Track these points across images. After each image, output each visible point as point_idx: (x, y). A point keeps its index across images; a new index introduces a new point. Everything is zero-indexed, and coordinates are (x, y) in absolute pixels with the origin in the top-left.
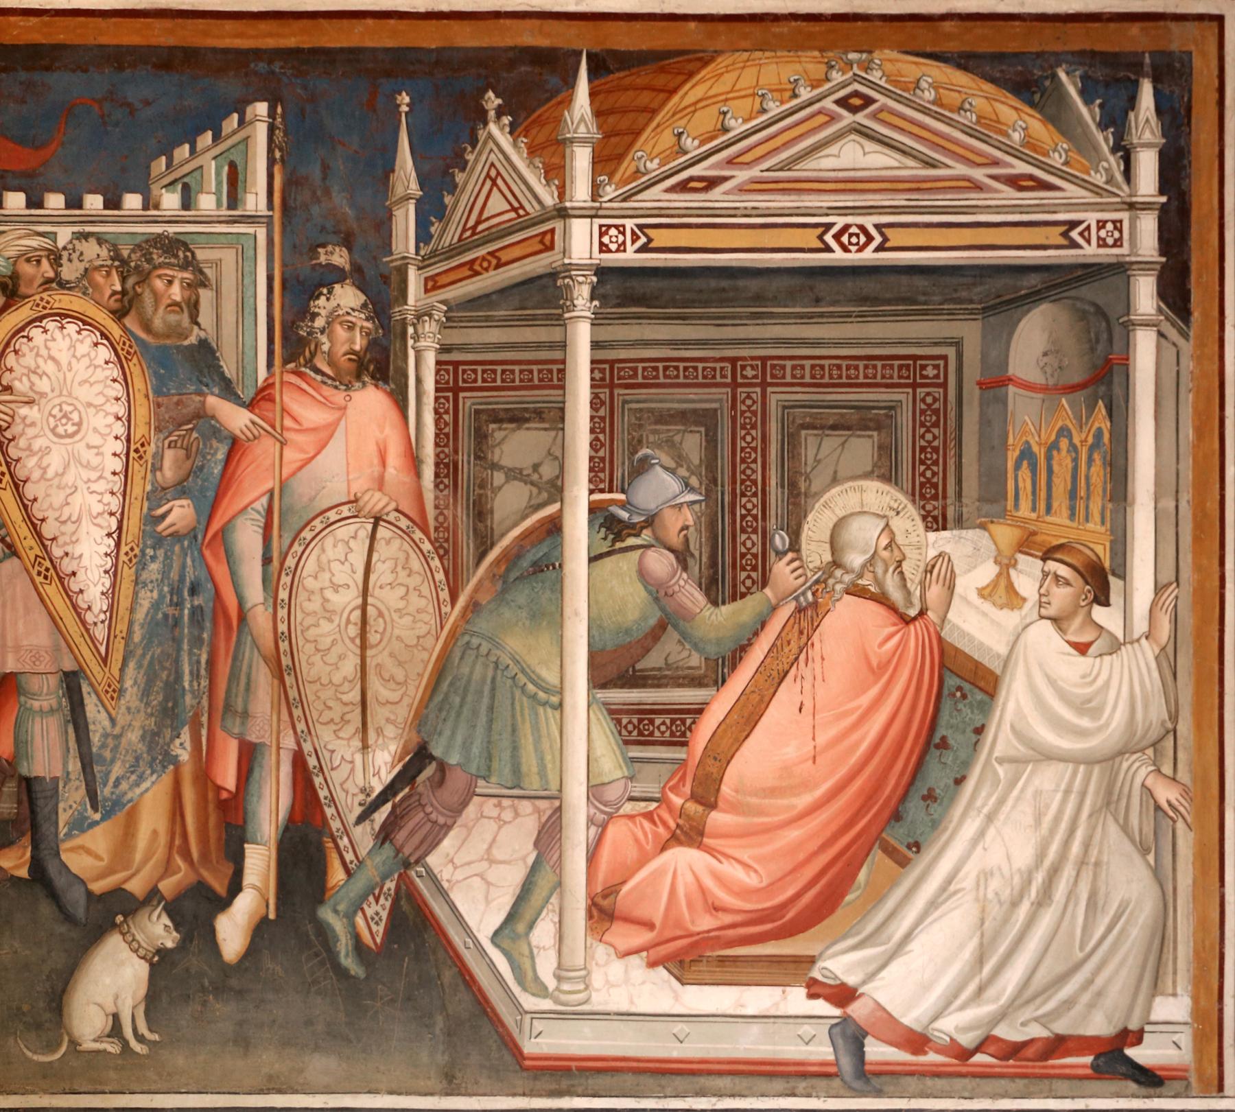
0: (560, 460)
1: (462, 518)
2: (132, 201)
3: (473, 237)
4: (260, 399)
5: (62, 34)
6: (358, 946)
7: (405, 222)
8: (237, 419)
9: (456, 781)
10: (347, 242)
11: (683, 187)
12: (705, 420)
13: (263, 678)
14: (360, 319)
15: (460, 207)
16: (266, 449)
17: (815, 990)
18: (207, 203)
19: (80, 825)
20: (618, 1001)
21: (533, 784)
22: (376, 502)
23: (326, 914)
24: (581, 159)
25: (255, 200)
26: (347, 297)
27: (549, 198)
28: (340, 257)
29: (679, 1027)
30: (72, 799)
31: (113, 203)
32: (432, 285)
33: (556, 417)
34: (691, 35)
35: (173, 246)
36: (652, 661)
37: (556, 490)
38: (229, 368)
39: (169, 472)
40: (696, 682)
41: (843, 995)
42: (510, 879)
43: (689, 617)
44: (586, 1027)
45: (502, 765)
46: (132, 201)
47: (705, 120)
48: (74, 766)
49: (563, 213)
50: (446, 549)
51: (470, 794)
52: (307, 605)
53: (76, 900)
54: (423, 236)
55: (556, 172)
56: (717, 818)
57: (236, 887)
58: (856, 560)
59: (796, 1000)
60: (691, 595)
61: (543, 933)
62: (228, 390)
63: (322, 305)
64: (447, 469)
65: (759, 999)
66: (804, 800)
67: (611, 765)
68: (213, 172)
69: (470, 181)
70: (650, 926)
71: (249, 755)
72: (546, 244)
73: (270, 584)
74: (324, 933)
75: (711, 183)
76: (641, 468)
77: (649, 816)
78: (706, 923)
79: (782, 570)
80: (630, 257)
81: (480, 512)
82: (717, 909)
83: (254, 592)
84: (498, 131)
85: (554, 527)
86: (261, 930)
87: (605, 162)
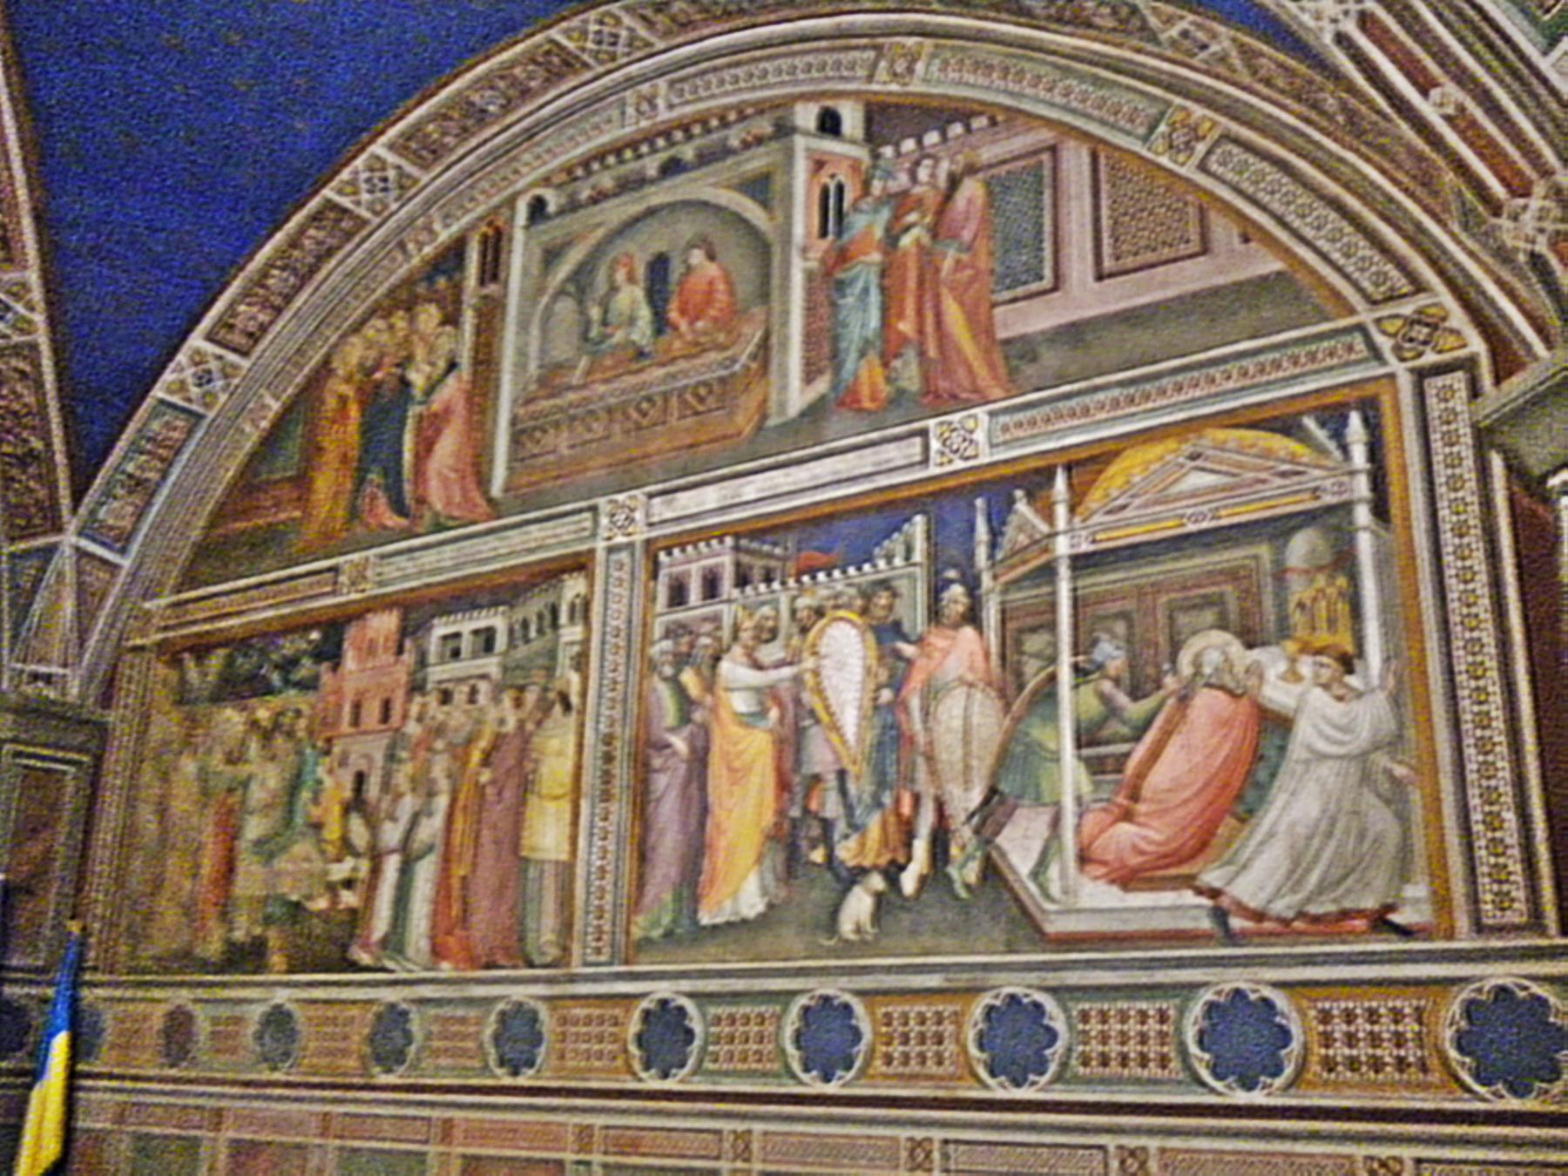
0: (1054, 645)
1: (1010, 678)
2: (867, 567)
3: (1014, 553)
4: (919, 641)
5: (840, 507)
6: (968, 887)
7: (981, 553)
8: (908, 650)
9: (1011, 801)
10: (955, 566)
11: (1110, 512)
12: (1124, 616)
13: (920, 761)
14: (964, 600)
15: (1006, 543)
16: (921, 663)
17: (1199, 892)
18: (898, 561)
19: (846, 837)
20: (1096, 904)
21: (1047, 799)
22: (970, 677)
23: (953, 871)
24: (1061, 511)
25: (918, 556)
26: (957, 590)
27: (1044, 528)
28: (952, 574)
29: (1125, 916)
30: (841, 827)
31: (859, 569)
32: (995, 577)
33: (1052, 627)
34: (1111, 446)
35: (885, 584)
36: (1106, 733)
37: (1053, 659)
38: (906, 627)
39: (883, 675)
40: (1125, 740)
41: (1214, 893)
42: (1036, 847)
43: (1122, 709)
44: (1074, 917)
45: (1031, 790)
46: (867, 567)
47: (1119, 481)
48: (841, 811)
49: (1053, 535)
50: (1002, 694)
51: (1015, 807)
52: (939, 730)
53: (844, 874)
54: (991, 556)
55: (1049, 517)
56: (1141, 808)
57: (909, 859)
58: (1207, 670)
59: (1189, 897)
60: (1122, 699)
61: (1053, 871)
62: (906, 639)
63: (946, 595)
64: (1003, 657)
65: (1167, 898)
66: (1187, 793)
67: (1086, 788)
68: (900, 550)
69: (1010, 531)
70: (1104, 863)
71: (917, 800)
72: (1046, 550)
73: (925, 721)
74: (949, 880)
75: (1124, 507)
76: (1095, 642)
77: (1104, 810)
78: (1135, 861)
79: (1170, 682)
80: (1085, 547)
81: (1019, 674)
82: (1142, 853)
83: (917, 725)
84: (1022, 507)
85: (1053, 678)
86: (923, 881)
87: (1072, 509)
